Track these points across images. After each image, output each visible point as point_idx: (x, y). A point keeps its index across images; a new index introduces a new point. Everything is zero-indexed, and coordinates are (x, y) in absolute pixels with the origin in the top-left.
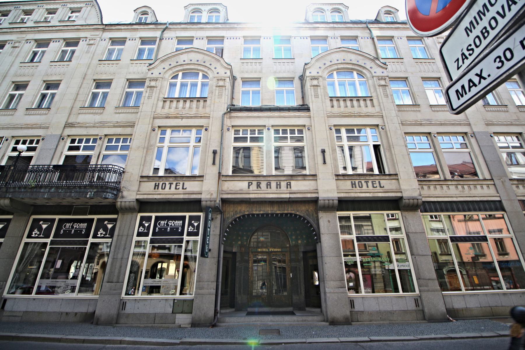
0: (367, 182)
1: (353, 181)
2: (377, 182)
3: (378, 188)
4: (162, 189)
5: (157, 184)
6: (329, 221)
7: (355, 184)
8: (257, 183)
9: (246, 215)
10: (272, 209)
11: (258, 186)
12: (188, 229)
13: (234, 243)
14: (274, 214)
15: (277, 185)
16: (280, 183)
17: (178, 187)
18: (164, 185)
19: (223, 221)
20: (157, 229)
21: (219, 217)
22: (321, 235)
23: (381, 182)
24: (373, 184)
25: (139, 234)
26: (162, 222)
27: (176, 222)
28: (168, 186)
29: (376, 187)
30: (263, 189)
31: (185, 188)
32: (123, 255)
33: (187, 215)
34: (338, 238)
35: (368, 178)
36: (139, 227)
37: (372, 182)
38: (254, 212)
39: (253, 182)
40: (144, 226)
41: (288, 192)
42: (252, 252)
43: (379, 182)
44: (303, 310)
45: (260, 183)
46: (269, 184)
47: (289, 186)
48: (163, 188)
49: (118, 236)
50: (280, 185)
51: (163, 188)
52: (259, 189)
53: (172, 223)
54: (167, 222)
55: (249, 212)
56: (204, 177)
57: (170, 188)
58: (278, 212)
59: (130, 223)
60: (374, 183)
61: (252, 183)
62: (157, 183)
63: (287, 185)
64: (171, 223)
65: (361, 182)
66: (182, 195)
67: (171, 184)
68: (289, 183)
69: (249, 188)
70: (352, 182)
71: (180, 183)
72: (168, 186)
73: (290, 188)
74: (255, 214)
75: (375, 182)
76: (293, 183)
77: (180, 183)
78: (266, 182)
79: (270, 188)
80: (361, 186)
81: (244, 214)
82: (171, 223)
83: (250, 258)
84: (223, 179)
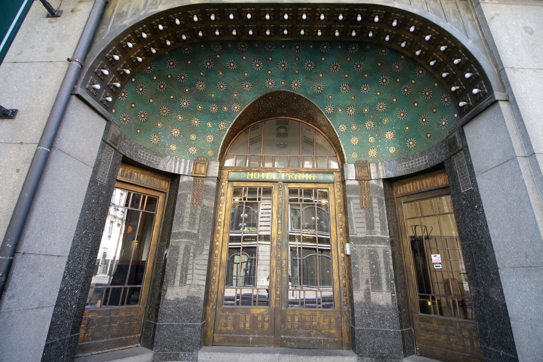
13: (173, 147)
83: (223, 195)
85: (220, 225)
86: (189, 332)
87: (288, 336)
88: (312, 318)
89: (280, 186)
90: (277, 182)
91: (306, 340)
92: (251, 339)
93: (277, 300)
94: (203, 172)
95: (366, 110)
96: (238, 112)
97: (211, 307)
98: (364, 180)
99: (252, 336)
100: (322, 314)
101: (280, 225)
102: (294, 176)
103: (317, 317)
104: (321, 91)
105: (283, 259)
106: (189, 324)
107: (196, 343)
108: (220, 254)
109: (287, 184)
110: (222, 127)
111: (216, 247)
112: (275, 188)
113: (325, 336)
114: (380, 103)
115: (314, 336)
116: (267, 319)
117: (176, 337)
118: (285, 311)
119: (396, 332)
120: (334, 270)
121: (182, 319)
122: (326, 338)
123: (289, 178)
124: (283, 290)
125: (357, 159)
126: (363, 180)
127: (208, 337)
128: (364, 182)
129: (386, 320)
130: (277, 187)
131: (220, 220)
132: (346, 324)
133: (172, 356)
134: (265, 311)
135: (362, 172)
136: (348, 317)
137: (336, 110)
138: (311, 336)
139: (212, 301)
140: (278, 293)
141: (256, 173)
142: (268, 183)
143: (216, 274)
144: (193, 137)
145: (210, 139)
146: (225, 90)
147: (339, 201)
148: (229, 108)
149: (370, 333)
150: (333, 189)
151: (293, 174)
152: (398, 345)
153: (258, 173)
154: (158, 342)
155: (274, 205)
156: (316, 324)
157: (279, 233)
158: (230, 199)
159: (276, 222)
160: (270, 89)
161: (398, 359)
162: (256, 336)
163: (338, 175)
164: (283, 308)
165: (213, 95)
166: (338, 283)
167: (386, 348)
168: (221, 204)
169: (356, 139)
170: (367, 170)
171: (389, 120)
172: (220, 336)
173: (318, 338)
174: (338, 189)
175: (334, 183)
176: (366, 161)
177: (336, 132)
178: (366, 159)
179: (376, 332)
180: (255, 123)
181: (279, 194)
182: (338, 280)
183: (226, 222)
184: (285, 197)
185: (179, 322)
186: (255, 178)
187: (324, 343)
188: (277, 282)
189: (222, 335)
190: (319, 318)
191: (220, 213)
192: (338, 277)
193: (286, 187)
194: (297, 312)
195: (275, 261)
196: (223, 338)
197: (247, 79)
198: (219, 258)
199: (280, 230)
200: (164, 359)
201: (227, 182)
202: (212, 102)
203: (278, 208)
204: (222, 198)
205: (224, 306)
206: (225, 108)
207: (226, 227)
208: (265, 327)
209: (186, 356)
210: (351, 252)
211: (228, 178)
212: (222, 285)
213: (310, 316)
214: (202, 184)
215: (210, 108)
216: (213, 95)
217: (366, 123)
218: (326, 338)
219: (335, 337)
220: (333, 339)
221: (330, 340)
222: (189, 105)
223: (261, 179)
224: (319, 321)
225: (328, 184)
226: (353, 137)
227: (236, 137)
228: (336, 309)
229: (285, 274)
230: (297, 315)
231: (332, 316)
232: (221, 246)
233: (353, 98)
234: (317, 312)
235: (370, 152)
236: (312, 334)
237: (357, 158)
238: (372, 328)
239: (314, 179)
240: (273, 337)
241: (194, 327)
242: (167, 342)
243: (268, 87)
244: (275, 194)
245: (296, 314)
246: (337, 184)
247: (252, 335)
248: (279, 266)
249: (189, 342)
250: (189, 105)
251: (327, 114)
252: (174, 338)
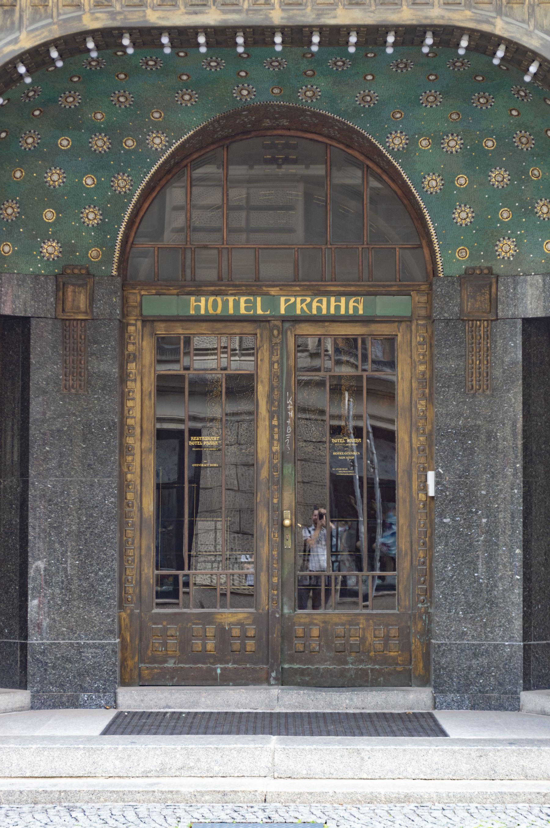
9: (93, 33)
14: (310, 29)
42: (146, 321)
44: (501, 707)
55: (113, 15)
74: (161, 30)
81: (73, 28)
83: (134, 357)
85: (133, 435)
86: (93, 657)
87: (297, 663)
88: (350, 630)
89: (275, 332)
90: (268, 321)
91: (336, 670)
92: (219, 671)
93: (274, 595)
94: (82, 306)
95: (490, 144)
96: (163, 151)
97: (129, 611)
98: (480, 320)
99: (222, 666)
100: (371, 621)
101: (276, 430)
102: (309, 306)
103: (361, 626)
104: (372, 105)
105: (285, 508)
106: (91, 641)
107: (110, 677)
108: (139, 501)
109: (293, 326)
110: (122, 185)
111: (128, 486)
112: (261, 336)
113: (375, 662)
114: (521, 132)
115: (352, 664)
116: (251, 633)
117: (68, 666)
118: (290, 618)
119: (513, 645)
120: (402, 529)
121: (74, 634)
122: (377, 667)
123: (298, 312)
124: (286, 572)
125: (469, 264)
126: (477, 320)
127: (129, 670)
128: (480, 326)
129: (498, 624)
130: (266, 333)
131: (130, 422)
132: (420, 638)
133: (64, 699)
134: (247, 618)
135: (476, 300)
136: (425, 624)
137: (412, 142)
138: (346, 663)
139: (130, 600)
140: (275, 580)
141: (211, 299)
142: (245, 324)
143: (133, 543)
144: (49, 215)
145: (91, 216)
146: (130, 105)
147: (422, 368)
148: (141, 143)
149: (462, 651)
150: (409, 336)
151: (309, 300)
152: (515, 668)
153: (219, 299)
154: (34, 674)
155: (262, 382)
156: (357, 640)
157: (274, 449)
158: (150, 367)
159: (267, 423)
160: (245, 102)
161: (512, 694)
162: (230, 666)
163: (424, 299)
164: (286, 611)
165: (99, 116)
166: (409, 558)
167: (493, 676)
168: (129, 383)
169: (467, 210)
170: (487, 297)
171: (544, 174)
172: (152, 669)
173: (360, 667)
174: (420, 336)
175: (411, 321)
176: (490, 269)
177: (416, 195)
178: (489, 265)
179: (476, 649)
180: (202, 152)
181: (271, 354)
182: (409, 552)
183: (145, 426)
184: (288, 359)
185: (71, 639)
186: (211, 311)
187: (372, 676)
188: (273, 559)
189: (156, 665)
190: (364, 629)
191: (130, 404)
192: (408, 545)
193: (289, 333)
194: (315, 619)
195: (265, 514)
196: (159, 671)
197: (187, 85)
198: (135, 508)
199: (275, 443)
200: (50, 705)
201: (139, 324)
202: (95, 129)
203: (272, 388)
204: (132, 367)
205: (156, 611)
206: (130, 143)
207: (146, 437)
208: (248, 648)
209: (91, 698)
210: (436, 492)
211: (141, 315)
212: (148, 568)
213: (343, 624)
214: (83, 337)
215: (90, 143)
216: (99, 116)
217: (490, 173)
218: (377, 667)
219: (397, 664)
220: (392, 668)
221: (387, 668)
222: (39, 141)
223: (226, 314)
224: (364, 635)
225: (396, 324)
226: (460, 206)
227: (154, 194)
228: (402, 610)
229: (290, 541)
230: (316, 625)
231: (392, 625)
232: (138, 482)
233: (454, 116)
234: (361, 617)
235: (501, 245)
236: (349, 659)
237: (467, 260)
238: (468, 640)
239: (361, 312)
240: (265, 666)
241: (102, 647)
242: (51, 676)
243: (238, 99)
244: (262, 352)
245: (315, 621)
246: (417, 325)
247: (221, 664)
248: (275, 523)
249: (96, 675)
250: (39, 141)
251: (391, 152)
252: (64, 667)
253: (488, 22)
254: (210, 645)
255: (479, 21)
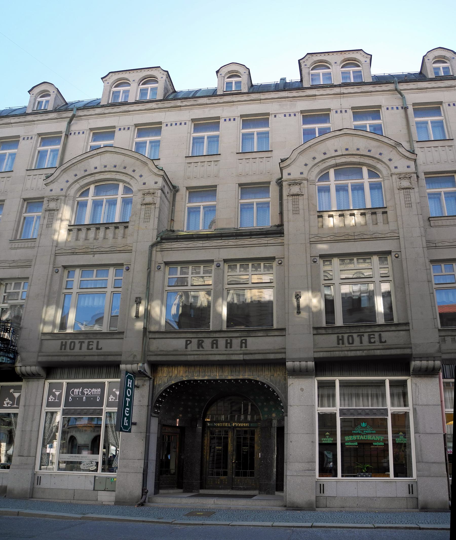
0: (361, 337)
1: (340, 335)
2: (377, 335)
3: (377, 343)
4: (70, 349)
5: (64, 343)
6: (302, 390)
7: (343, 339)
8: (199, 341)
10: (220, 374)
11: (200, 345)
12: (108, 399)
15: (227, 343)
16: (231, 340)
17: (90, 347)
18: (73, 344)
19: (153, 388)
20: (70, 398)
21: (147, 384)
22: (289, 407)
23: (383, 334)
24: (370, 338)
25: (49, 404)
26: (76, 391)
27: (93, 390)
28: (78, 346)
29: (374, 342)
30: (206, 348)
31: (100, 347)
32: (32, 427)
33: (106, 381)
34: (313, 412)
35: (362, 330)
36: (49, 397)
37: (369, 336)
38: (196, 378)
39: (193, 340)
40: (54, 395)
41: (241, 352)
43: (380, 335)
45: (203, 341)
46: (215, 342)
47: (244, 345)
48: (72, 348)
49: (24, 406)
50: (231, 343)
51: (72, 348)
52: (201, 349)
53: (89, 391)
54: (82, 390)
56: (125, 334)
57: (81, 348)
58: (230, 378)
59: (37, 391)
60: (372, 336)
61: (191, 342)
62: (64, 341)
63: (242, 343)
64: (87, 391)
65: (352, 336)
66: (96, 357)
67: (81, 343)
68: (244, 341)
69: (186, 348)
70: (338, 337)
71: (93, 342)
72: (78, 346)
73: (246, 347)
75: (374, 335)
76: (250, 340)
77: (93, 342)
78: (210, 340)
79: (217, 347)
80: (351, 342)
82: (87, 391)
84: (151, 336)
253: (256, 378)
254: (219, 483)
255: (254, 378)
